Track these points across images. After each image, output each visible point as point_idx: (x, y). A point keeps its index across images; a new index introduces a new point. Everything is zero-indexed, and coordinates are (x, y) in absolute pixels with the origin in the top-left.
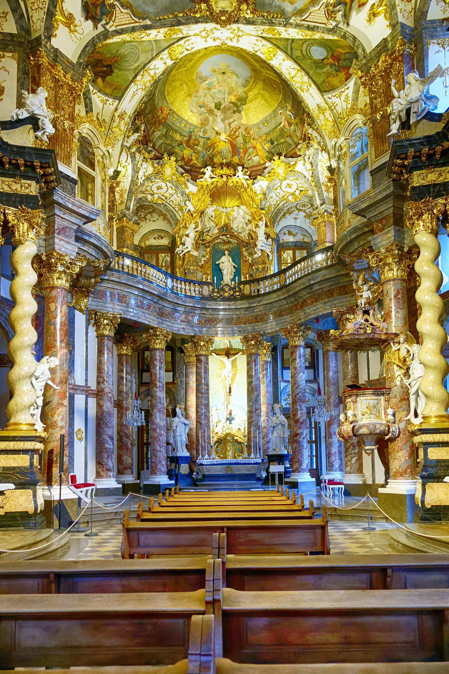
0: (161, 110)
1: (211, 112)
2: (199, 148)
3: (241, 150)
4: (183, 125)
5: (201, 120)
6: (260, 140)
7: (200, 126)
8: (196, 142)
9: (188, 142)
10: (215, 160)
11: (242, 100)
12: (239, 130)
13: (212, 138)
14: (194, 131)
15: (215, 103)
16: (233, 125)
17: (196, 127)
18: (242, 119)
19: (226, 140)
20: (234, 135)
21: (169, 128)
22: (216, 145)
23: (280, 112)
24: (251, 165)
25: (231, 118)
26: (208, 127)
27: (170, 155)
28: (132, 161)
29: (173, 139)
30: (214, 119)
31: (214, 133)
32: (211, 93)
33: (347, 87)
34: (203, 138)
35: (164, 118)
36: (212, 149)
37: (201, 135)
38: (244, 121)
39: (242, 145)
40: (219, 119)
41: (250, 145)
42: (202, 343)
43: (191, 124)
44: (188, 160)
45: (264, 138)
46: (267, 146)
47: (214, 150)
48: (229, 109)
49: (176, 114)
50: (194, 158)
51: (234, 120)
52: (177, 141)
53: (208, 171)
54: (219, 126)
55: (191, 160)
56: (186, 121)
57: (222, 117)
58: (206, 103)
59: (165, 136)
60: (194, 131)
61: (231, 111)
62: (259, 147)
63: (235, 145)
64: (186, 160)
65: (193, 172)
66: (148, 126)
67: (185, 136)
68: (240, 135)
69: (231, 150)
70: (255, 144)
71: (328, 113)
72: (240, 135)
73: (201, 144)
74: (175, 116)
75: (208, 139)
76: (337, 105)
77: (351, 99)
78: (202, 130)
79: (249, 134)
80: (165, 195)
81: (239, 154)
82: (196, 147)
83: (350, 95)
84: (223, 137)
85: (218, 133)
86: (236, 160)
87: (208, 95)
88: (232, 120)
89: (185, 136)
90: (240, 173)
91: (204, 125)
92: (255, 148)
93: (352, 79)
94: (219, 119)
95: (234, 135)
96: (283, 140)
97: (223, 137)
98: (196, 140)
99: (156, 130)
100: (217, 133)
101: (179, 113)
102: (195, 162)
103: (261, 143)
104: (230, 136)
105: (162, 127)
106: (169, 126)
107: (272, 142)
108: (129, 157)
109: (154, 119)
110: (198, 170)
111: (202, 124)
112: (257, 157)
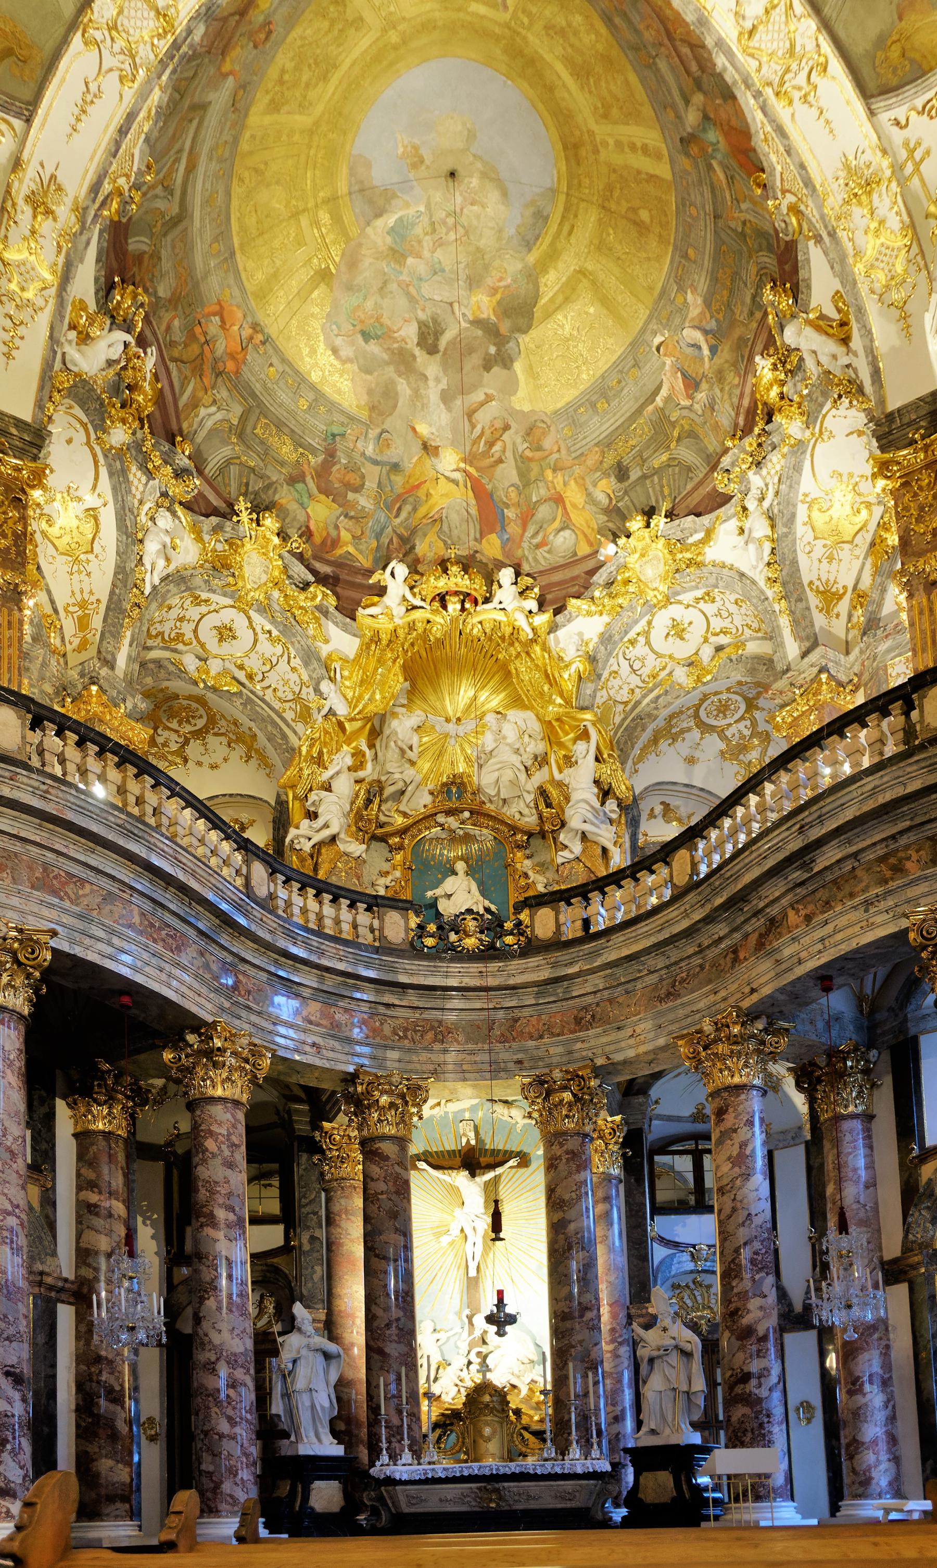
0: (220, 313)
1: (403, 361)
2: (364, 501)
3: (510, 513)
4: (303, 404)
5: (370, 392)
6: (577, 470)
7: (364, 415)
8: (353, 478)
9: (322, 473)
10: (422, 548)
13: (409, 465)
14: (343, 435)
15: (422, 325)
16: (484, 417)
17: (352, 418)
19: (457, 476)
20: (486, 454)
21: (255, 407)
22: (421, 493)
24: (544, 565)
25: (474, 387)
26: (394, 423)
27: (259, 508)
28: (115, 490)
29: (266, 453)
30: (417, 394)
31: (417, 448)
32: (404, 277)
34: (376, 463)
35: (232, 357)
36: (408, 508)
37: (370, 450)
38: (522, 401)
39: (513, 494)
40: (433, 393)
41: (543, 492)
43: (332, 406)
44: (324, 542)
45: (592, 460)
46: (605, 489)
47: (415, 509)
48: (471, 351)
49: (277, 350)
50: (345, 536)
52: (282, 464)
54: (434, 422)
56: (313, 387)
58: (385, 320)
59: (241, 432)
60: (343, 435)
61: (475, 360)
63: (491, 495)
64: (317, 539)
65: (346, 585)
66: (172, 366)
67: (314, 451)
68: (509, 454)
69: (474, 511)
70: (560, 487)
72: (509, 454)
73: (371, 485)
74: (275, 360)
75: (395, 467)
78: (373, 433)
79: (539, 448)
80: (247, 663)
81: (503, 528)
82: (351, 496)
84: (449, 461)
85: (429, 449)
86: (492, 547)
87: (393, 286)
88: (479, 396)
89: (314, 451)
90: (506, 593)
91: (381, 414)
92: (559, 500)
95: (486, 454)
98: (353, 468)
99: (207, 399)
100: (425, 446)
101: (289, 351)
103: (581, 482)
104: (469, 459)
105: (225, 394)
106: (253, 395)
107: (621, 473)
108: (103, 472)
109: (195, 349)
110: (359, 579)
111: (373, 408)
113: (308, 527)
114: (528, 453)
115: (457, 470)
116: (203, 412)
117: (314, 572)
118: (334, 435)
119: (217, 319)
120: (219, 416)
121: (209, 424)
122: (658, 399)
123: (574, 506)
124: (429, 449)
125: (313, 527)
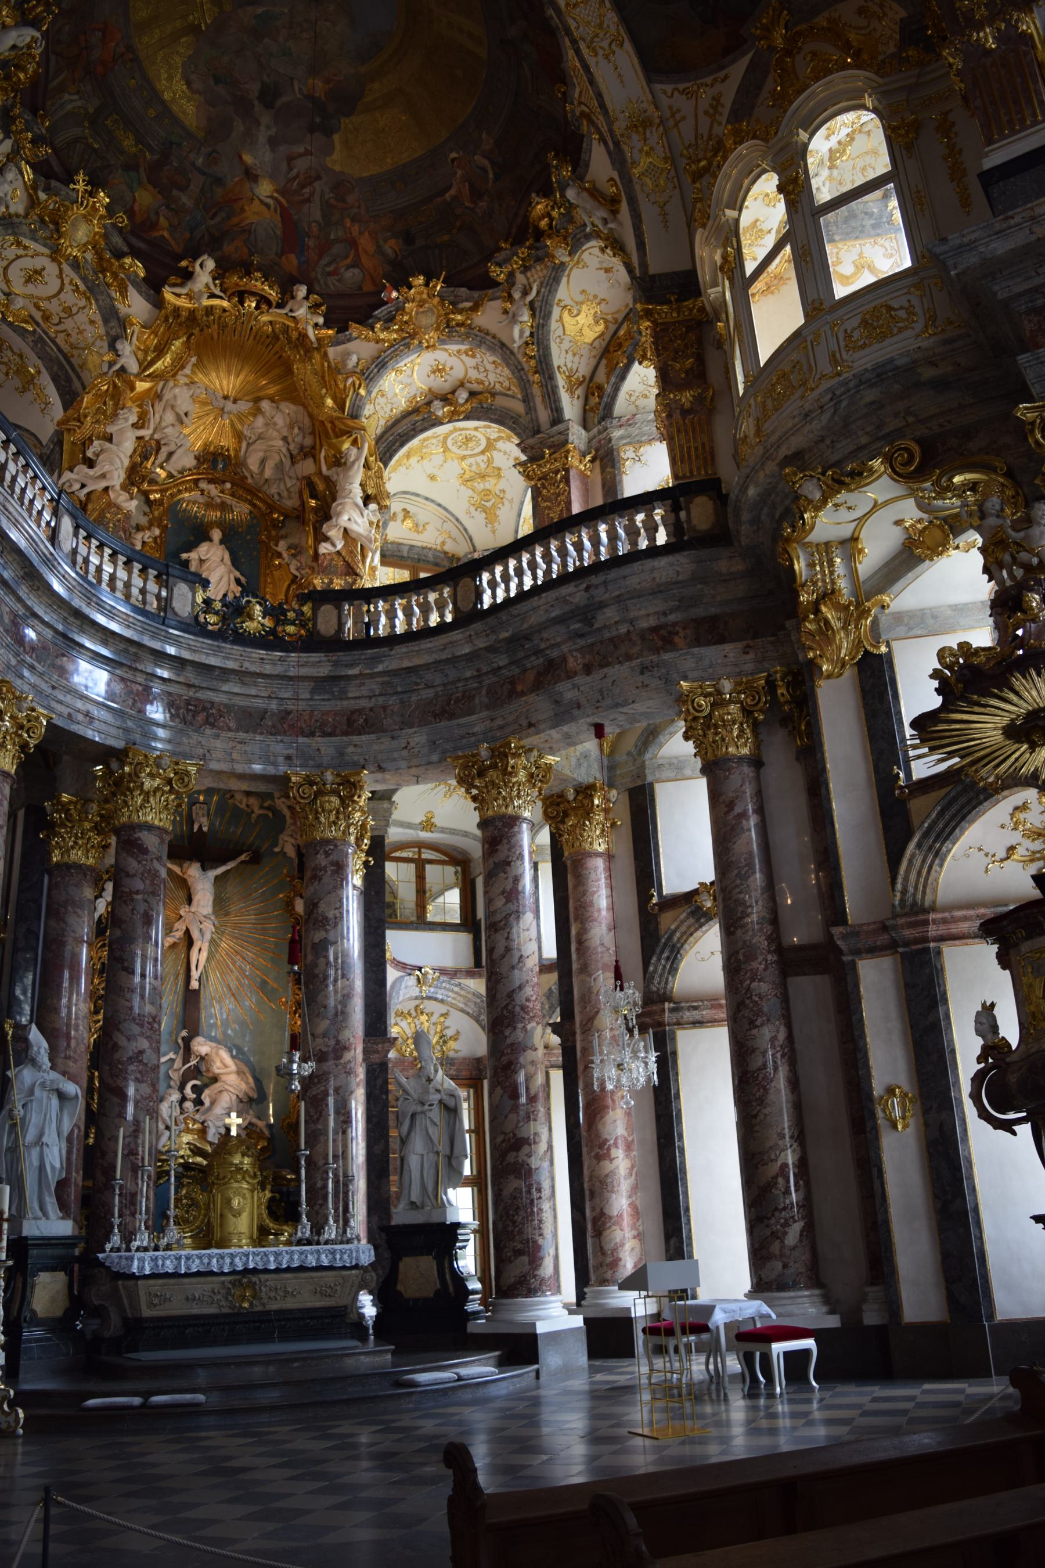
2: (186, 200)
3: (311, 243)
4: (152, 113)
11: (345, 101)
12: (317, 184)
18: (331, 154)
19: (270, 201)
23: (453, 155)
27: (95, 183)
33: (721, 74)
34: (203, 173)
37: (200, 161)
38: (337, 161)
39: (315, 228)
41: (340, 233)
42: (148, 784)
46: (391, 246)
51: (307, 153)
53: (204, 271)
55: (154, 225)
56: (163, 103)
57: (273, 131)
62: (365, 243)
69: (279, 232)
71: (654, 136)
72: (317, 198)
75: (219, 181)
76: (684, 118)
77: (726, 111)
82: (175, 192)
83: (728, 101)
84: (265, 189)
92: (353, 243)
93: (744, 54)
94: (262, 136)
96: (446, 238)
97: (265, 189)
102: (166, 234)
104: (283, 192)
107: (408, 239)
112: (356, 271)
113: (132, 207)
114: (332, 201)
115: (271, 197)
116: (66, 97)
117: (129, 245)
118: (171, 143)
119: (99, 34)
120: (79, 103)
121: (69, 107)
122: (447, 195)
123: (366, 252)
124: (251, 176)
125: (136, 208)
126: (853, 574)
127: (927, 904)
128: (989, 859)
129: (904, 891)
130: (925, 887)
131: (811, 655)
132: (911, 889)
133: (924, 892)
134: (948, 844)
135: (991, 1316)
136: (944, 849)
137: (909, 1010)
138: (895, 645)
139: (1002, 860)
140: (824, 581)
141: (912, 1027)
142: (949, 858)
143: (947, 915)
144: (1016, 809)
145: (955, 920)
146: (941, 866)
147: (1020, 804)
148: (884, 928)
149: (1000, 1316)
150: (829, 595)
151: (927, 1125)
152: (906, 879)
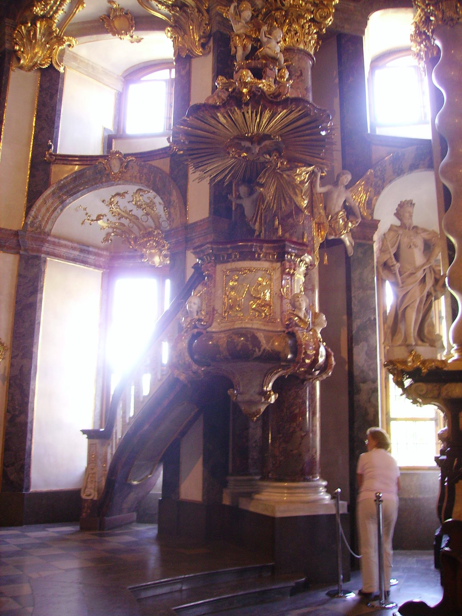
126: (69, 14)
127: (47, 230)
128: (86, 217)
129: (35, 217)
130: (48, 219)
131: (17, 48)
132: (40, 218)
133: (47, 222)
134: (70, 199)
135: (28, 488)
136: (68, 201)
137: (17, 292)
138: (67, 69)
139: (92, 220)
140: (51, 8)
141: (17, 302)
142: (67, 207)
143: (57, 240)
144: (118, 194)
145: (60, 245)
146: (62, 210)
147: (122, 192)
148: (16, 234)
149: (32, 490)
150: (47, 18)
151: (12, 365)
152: (39, 210)
